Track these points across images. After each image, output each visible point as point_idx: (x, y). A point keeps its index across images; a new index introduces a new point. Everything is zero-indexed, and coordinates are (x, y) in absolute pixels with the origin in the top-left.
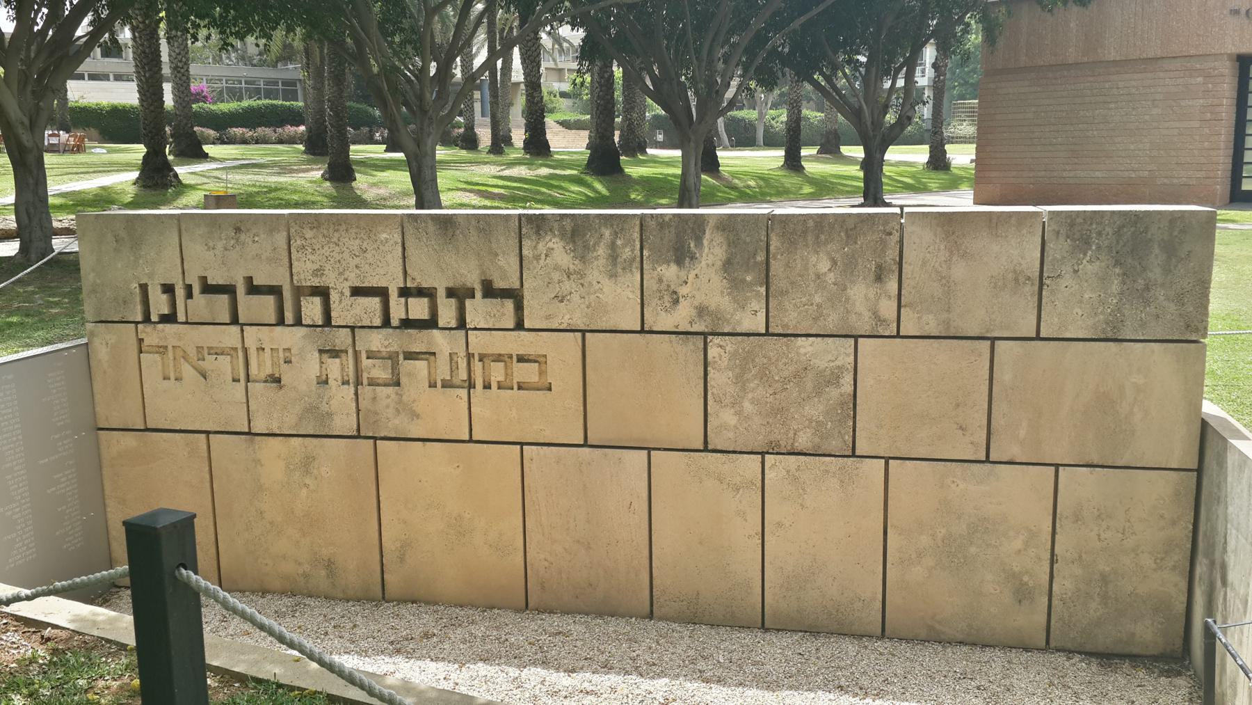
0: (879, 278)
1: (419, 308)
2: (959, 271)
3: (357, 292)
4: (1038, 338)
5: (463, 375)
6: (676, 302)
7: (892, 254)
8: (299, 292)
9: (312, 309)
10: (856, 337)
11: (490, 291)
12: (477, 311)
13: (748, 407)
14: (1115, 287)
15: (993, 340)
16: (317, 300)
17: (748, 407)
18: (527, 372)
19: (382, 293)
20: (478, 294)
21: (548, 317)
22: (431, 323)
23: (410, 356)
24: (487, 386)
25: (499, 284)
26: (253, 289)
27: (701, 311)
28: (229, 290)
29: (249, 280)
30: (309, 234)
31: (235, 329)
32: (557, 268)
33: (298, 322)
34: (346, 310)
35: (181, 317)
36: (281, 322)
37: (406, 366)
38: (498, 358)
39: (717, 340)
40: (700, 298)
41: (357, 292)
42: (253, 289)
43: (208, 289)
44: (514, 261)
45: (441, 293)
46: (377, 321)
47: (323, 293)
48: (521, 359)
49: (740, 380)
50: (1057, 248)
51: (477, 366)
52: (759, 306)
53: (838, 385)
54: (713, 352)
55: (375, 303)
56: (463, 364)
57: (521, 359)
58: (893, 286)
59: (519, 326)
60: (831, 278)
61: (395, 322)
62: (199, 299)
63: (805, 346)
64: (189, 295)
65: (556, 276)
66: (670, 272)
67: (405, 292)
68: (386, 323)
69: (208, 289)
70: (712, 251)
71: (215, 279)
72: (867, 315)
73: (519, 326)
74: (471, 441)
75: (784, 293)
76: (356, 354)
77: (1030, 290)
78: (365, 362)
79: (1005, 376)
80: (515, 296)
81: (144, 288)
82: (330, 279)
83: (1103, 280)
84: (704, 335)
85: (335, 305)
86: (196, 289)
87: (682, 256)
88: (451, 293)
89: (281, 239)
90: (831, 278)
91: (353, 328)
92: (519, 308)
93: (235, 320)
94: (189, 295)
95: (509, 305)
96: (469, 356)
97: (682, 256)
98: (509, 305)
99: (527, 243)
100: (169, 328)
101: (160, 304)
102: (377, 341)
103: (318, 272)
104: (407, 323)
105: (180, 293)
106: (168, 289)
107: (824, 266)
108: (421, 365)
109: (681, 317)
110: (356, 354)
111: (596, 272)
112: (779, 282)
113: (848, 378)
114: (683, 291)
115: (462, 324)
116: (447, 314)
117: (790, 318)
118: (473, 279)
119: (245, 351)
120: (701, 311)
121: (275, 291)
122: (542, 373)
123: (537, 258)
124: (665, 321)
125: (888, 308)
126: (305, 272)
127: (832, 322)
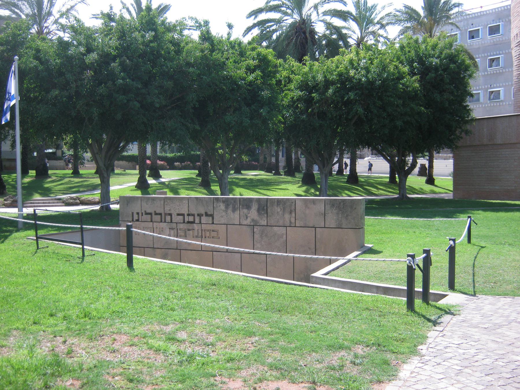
0: (291, 213)
1: (191, 219)
2: (307, 212)
3: (178, 215)
4: (325, 227)
5: (200, 234)
6: (247, 218)
7: (293, 207)
8: (166, 214)
9: (168, 218)
10: (286, 227)
11: (207, 215)
12: (204, 219)
13: (263, 242)
14: (340, 216)
15: (315, 228)
16: (169, 217)
17: (263, 242)
18: (214, 234)
19: (183, 215)
20: (204, 215)
21: (219, 221)
22: (193, 222)
23: (189, 230)
24: (205, 237)
25: (209, 213)
26: (156, 214)
27: (253, 220)
28: (150, 214)
29: (155, 212)
30: (168, 201)
31: (152, 223)
32: (221, 209)
33: (165, 222)
34: (176, 219)
35: (140, 220)
36: (161, 222)
37: (188, 232)
38: (208, 231)
39: (256, 227)
40: (252, 217)
41: (178, 215)
42: (156, 214)
43: (147, 214)
44: (212, 208)
45: (196, 215)
46: (182, 222)
47: (170, 215)
48: (213, 231)
49: (261, 236)
50: (328, 207)
51: (203, 233)
52: (265, 219)
53: (282, 238)
54: (255, 230)
55: (181, 217)
56: (200, 232)
57: (213, 231)
58: (293, 215)
59: (213, 223)
60: (281, 213)
61: (186, 222)
62: (144, 216)
63: (275, 228)
64: (142, 215)
65: (221, 211)
66: (245, 211)
67: (188, 215)
68: (184, 222)
69: (147, 214)
70: (255, 207)
71: (149, 211)
72: (288, 222)
73: (213, 223)
74: (201, 250)
75: (270, 216)
76: (177, 229)
77: (322, 217)
78: (179, 231)
79: (318, 236)
80: (212, 216)
81: (133, 213)
82: (172, 212)
83: (338, 214)
84: (254, 226)
85: (173, 218)
86: (144, 214)
87: (248, 207)
88: (198, 215)
89: (162, 202)
90: (281, 213)
91: (177, 223)
92: (213, 219)
93: (152, 221)
94: (142, 215)
95: (211, 218)
96: (202, 230)
97: (248, 207)
98: (211, 218)
99: (215, 204)
100: (137, 223)
101: (136, 217)
102: (181, 226)
103: (170, 210)
104: (189, 222)
105: (140, 214)
106: (138, 214)
107: (279, 210)
108: (191, 232)
109: (248, 221)
110: (177, 229)
111: (230, 211)
112: (269, 214)
113: (285, 236)
114: (249, 215)
115: (200, 223)
116: (197, 220)
117: (272, 222)
118: (203, 212)
119: (153, 228)
120: (253, 220)
121: (160, 214)
122: (217, 234)
123: (217, 207)
124: (245, 222)
125: (293, 220)
126: (167, 209)
127: (281, 223)
